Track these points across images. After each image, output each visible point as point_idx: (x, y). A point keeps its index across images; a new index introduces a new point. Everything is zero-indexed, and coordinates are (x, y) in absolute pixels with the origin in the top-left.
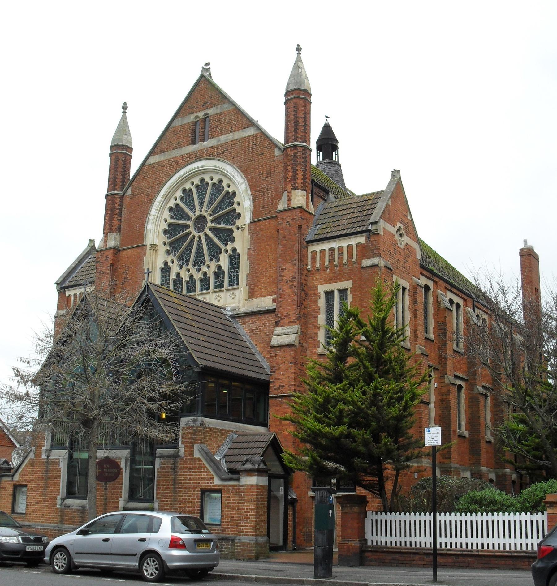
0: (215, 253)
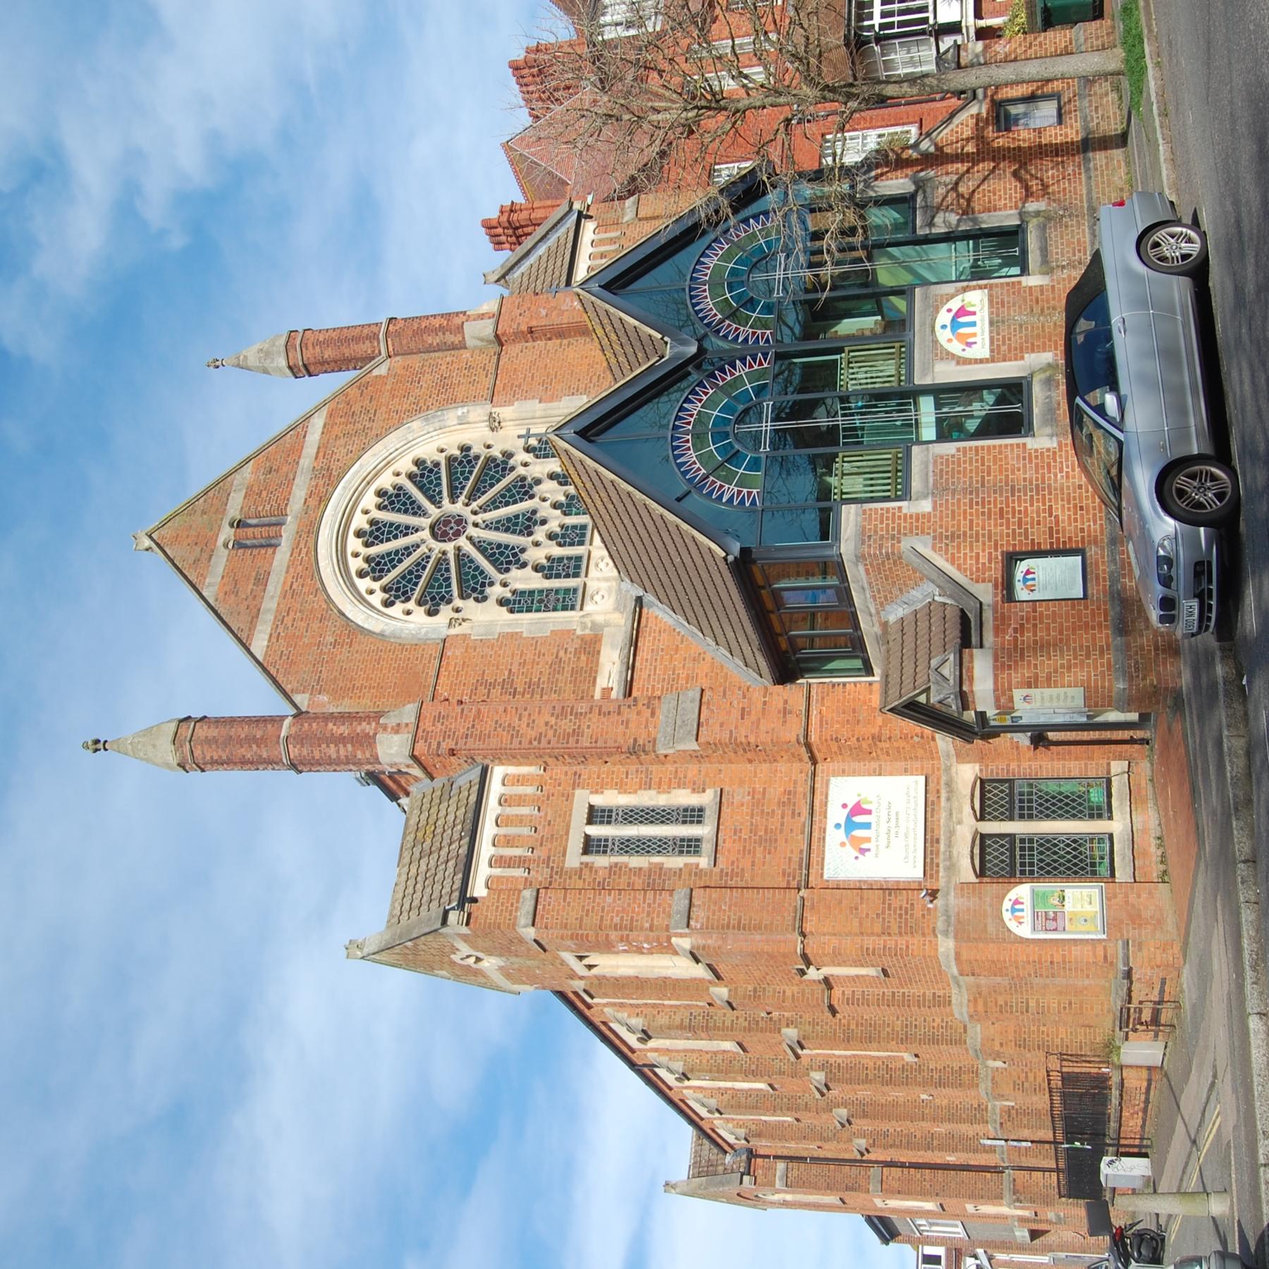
0: (524, 489)
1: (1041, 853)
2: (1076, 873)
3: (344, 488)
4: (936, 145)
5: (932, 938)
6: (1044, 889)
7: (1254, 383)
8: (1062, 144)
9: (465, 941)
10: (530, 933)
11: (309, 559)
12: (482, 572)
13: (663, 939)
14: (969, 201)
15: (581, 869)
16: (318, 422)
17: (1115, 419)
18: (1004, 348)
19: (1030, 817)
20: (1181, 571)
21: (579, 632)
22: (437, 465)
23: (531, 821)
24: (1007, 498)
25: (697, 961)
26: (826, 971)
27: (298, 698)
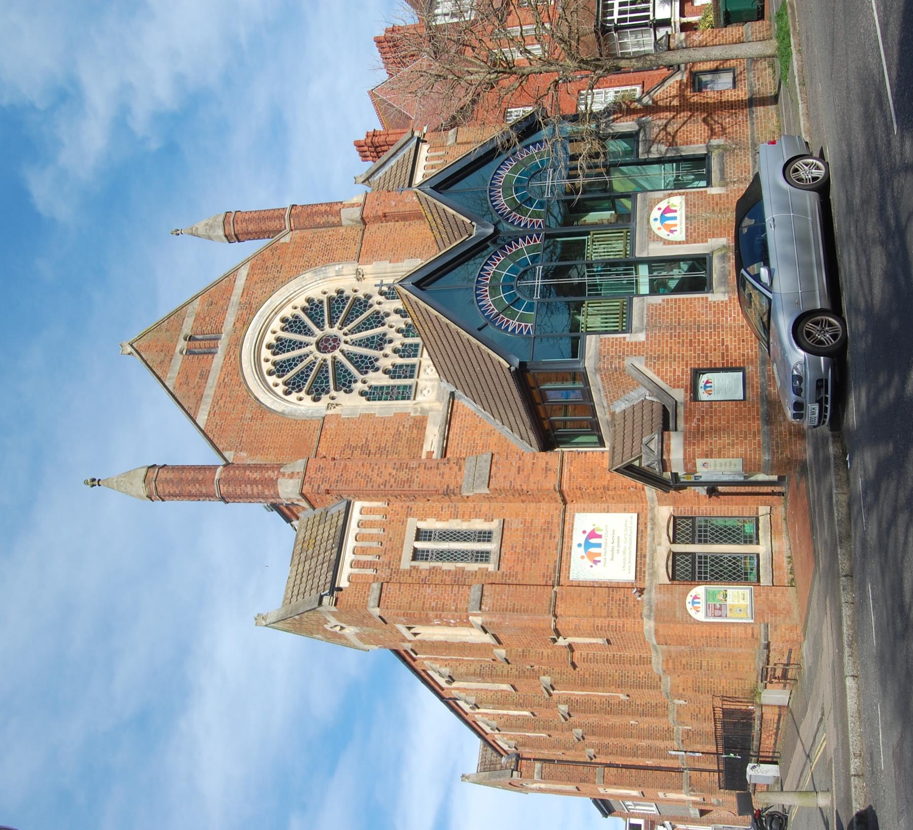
0: (378, 319)
1: (712, 565)
2: (734, 579)
3: (260, 316)
4: (653, 100)
5: (640, 621)
6: (713, 589)
7: (858, 264)
8: (735, 101)
9: (334, 616)
10: (376, 611)
11: (236, 363)
12: (350, 374)
13: (464, 617)
14: (674, 137)
15: (411, 570)
16: (244, 272)
17: (766, 284)
18: (695, 234)
19: (706, 542)
20: (808, 386)
21: (412, 414)
22: (321, 302)
23: (378, 538)
24: (695, 332)
25: (486, 632)
26: (570, 640)
27: (227, 454)
